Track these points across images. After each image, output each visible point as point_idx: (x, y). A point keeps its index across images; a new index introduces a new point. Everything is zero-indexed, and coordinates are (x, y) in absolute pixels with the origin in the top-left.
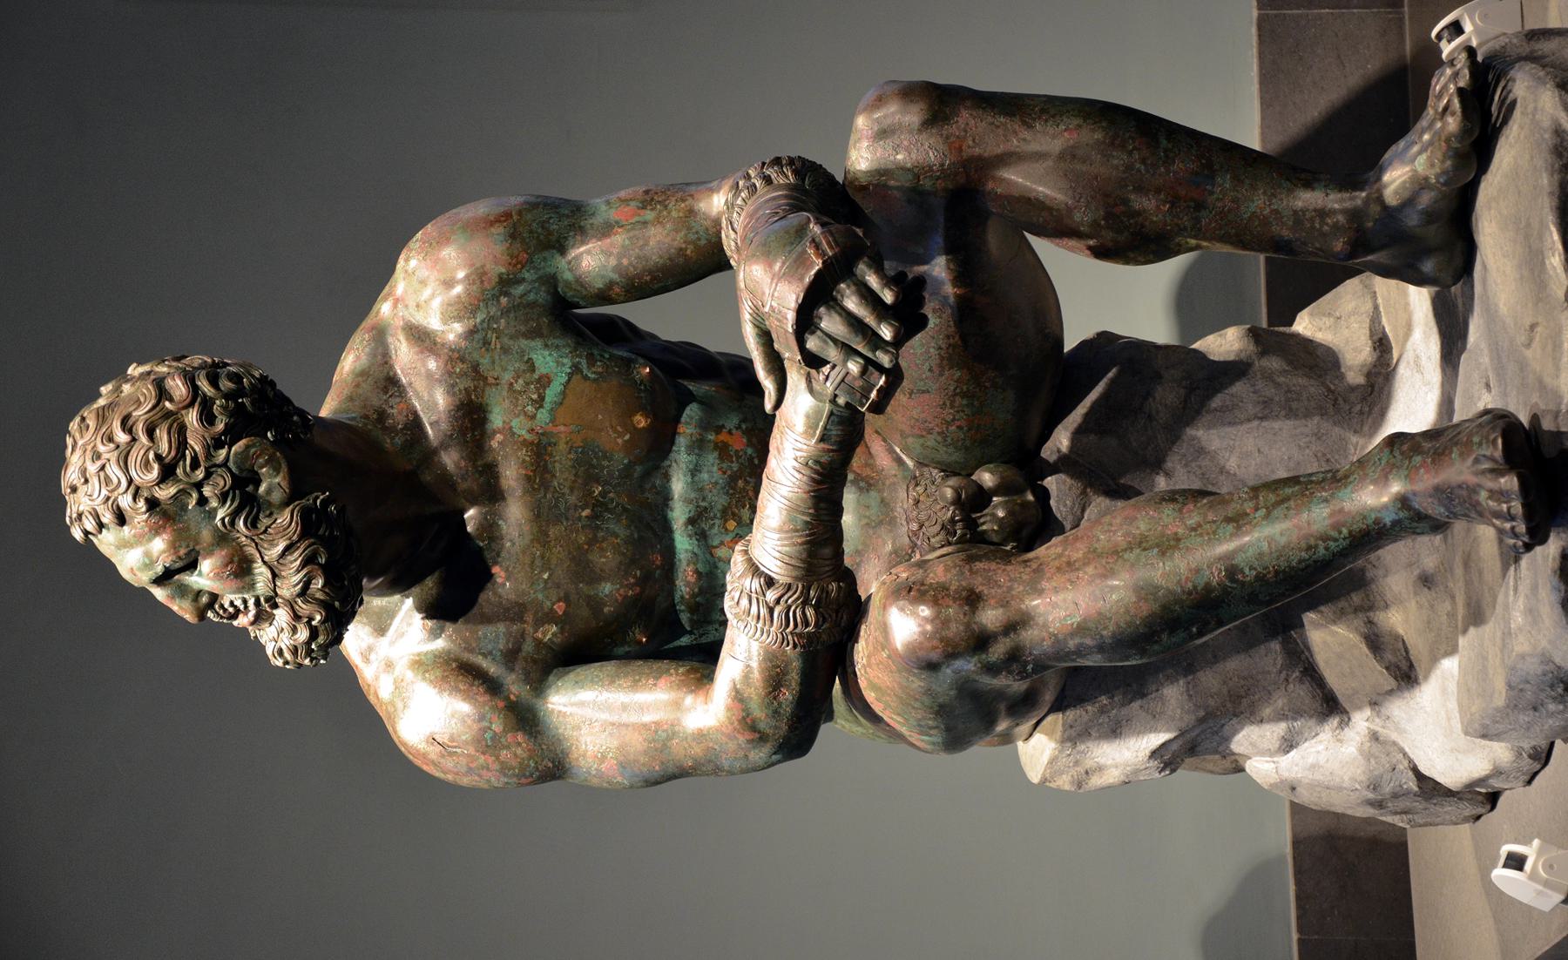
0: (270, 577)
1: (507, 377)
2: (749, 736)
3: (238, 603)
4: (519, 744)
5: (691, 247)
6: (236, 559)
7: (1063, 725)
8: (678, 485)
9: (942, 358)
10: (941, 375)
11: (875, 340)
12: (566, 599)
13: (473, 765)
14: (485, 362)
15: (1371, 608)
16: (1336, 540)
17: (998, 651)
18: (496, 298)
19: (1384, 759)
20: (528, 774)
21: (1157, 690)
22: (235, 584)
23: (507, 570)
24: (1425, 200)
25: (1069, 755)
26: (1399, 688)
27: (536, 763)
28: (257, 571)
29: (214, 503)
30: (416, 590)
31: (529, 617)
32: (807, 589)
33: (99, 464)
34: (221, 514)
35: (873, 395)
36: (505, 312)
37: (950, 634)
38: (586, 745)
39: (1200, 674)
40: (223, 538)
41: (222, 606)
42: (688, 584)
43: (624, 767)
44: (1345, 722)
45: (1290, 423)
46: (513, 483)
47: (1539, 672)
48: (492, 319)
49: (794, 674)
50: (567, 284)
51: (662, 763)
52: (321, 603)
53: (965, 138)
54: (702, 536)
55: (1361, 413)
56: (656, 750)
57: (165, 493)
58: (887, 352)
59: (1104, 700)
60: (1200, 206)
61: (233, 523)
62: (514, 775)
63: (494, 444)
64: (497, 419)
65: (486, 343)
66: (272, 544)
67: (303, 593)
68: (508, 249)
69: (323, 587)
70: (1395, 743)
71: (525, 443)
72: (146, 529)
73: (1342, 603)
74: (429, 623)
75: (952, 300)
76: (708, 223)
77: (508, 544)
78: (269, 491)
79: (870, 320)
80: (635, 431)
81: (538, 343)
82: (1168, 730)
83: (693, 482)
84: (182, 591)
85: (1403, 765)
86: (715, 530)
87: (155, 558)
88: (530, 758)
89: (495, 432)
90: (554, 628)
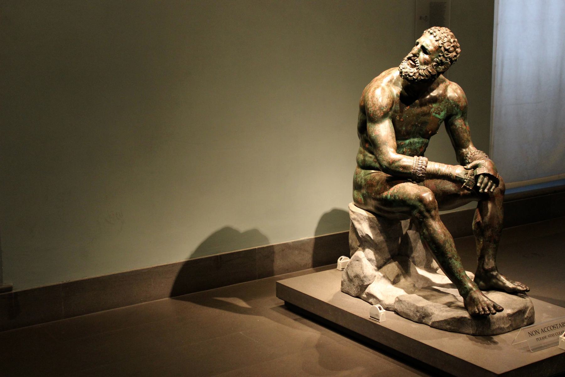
0: (424, 69)
1: (441, 107)
3: (418, 62)
5: (464, 142)
6: (428, 62)
7: (373, 217)
8: (416, 140)
9: (445, 191)
10: (441, 191)
11: (484, 188)
12: (403, 121)
13: (376, 105)
14: (443, 102)
15: (403, 275)
16: (460, 277)
17: (426, 214)
18: (455, 104)
19: (371, 278)
20: (374, 116)
21: (382, 235)
22: (422, 61)
23: (408, 109)
24: (500, 283)
25: (364, 218)
26: (391, 282)
28: (425, 66)
29: (440, 58)
30: (404, 91)
31: (401, 114)
32: (425, 174)
33: (447, 36)
34: (437, 59)
35: (468, 187)
36: (452, 106)
37: (430, 205)
39: (385, 243)
40: (432, 60)
41: (416, 59)
42: (401, 143)
44: (376, 270)
45: (425, 255)
46: (423, 109)
47: (429, 312)
48: (451, 103)
49: (406, 171)
50: (456, 117)
52: (417, 78)
53: (498, 197)
54: (408, 145)
55: (428, 268)
57: (442, 49)
58: (482, 190)
59: (379, 225)
60: (490, 242)
61: (435, 62)
62: (373, 113)
63: (430, 105)
64: (434, 105)
65: (446, 102)
66: (431, 69)
67: (420, 74)
68: (463, 106)
69: (421, 79)
70: (374, 280)
71: (430, 111)
73: (402, 269)
74: (399, 94)
75: (458, 193)
76: (468, 144)
77: (413, 109)
78: (439, 68)
79: (488, 187)
80: (429, 131)
81: (446, 112)
82: (373, 237)
83: (417, 142)
84: (419, 51)
85: (370, 282)
86: (408, 147)
88: (378, 116)
89: (432, 105)
90: (398, 119)
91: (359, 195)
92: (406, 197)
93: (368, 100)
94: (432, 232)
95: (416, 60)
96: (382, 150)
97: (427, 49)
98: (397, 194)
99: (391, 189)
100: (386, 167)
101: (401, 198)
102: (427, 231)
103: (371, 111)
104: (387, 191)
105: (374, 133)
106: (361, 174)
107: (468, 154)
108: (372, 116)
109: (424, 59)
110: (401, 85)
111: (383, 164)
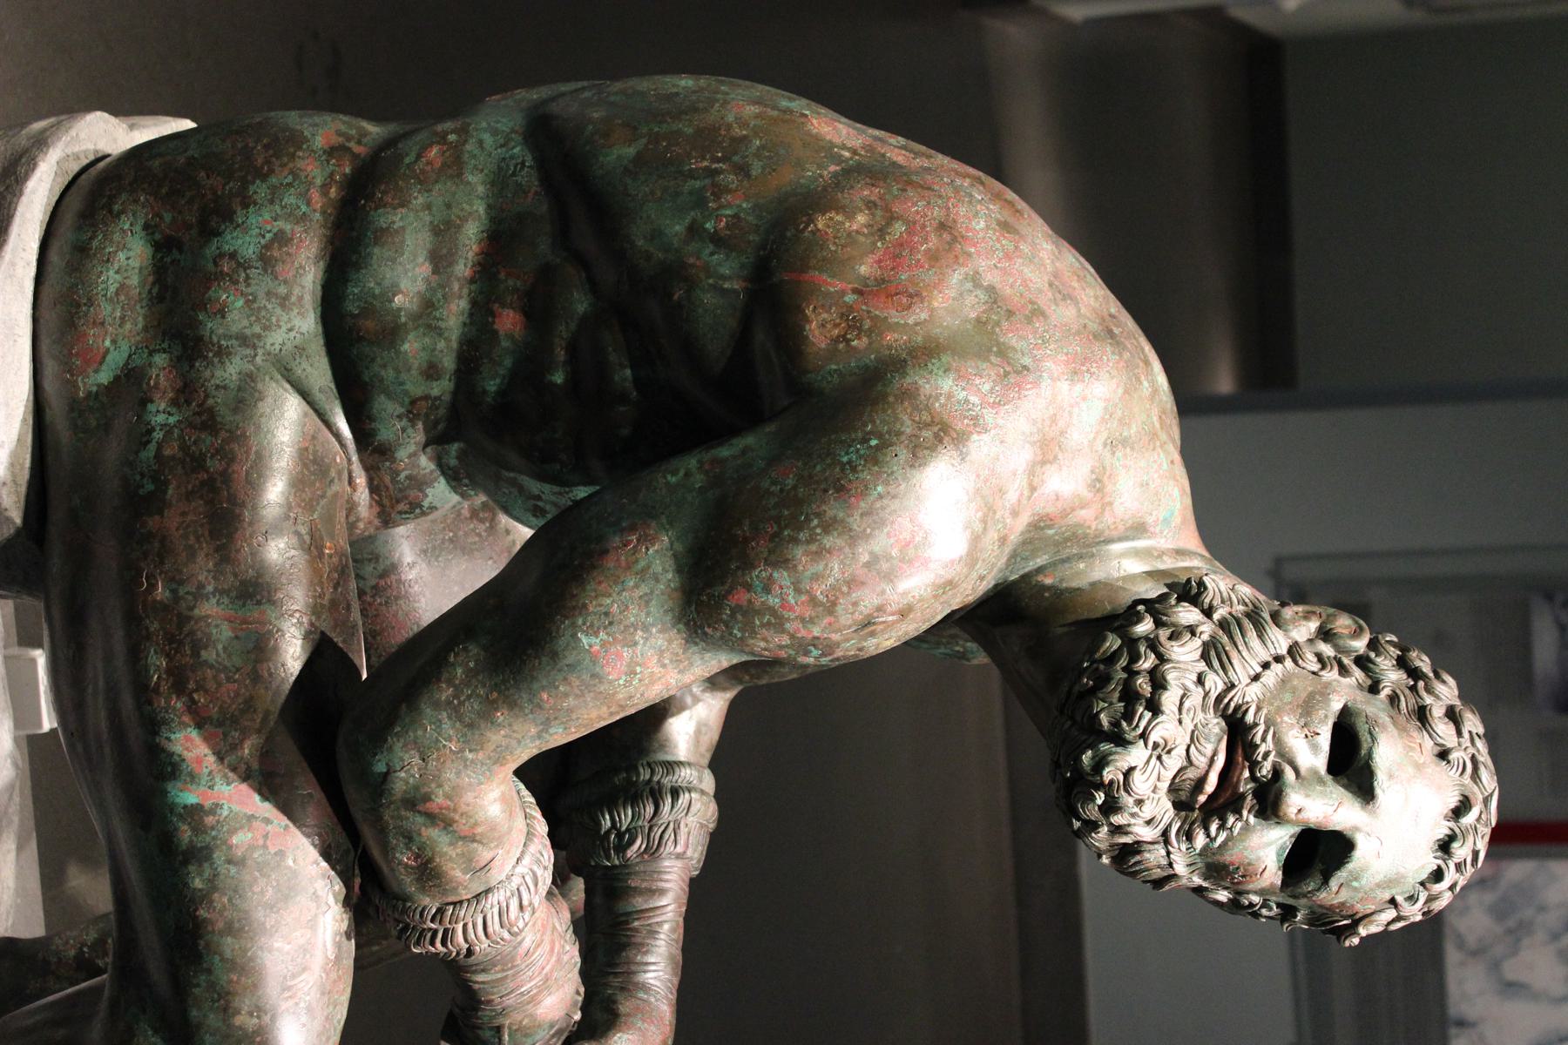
2: (432, 807)
4: (766, 649)
20: (739, 617)
22: (1229, 857)
27: (731, 634)
38: (664, 666)
43: (594, 676)
51: (540, 707)
56: (556, 718)
62: (759, 613)
87: (1343, 889)
91: (128, 326)
92: (223, 960)
93: (854, 539)
97: (1326, 881)
98: (222, 870)
99: (244, 787)
100: (386, 776)
101: (205, 920)
103: (767, 589)
104: (221, 759)
105: (604, 644)
106: (285, 318)
107: (675, 793)
108: (732, 602)
111: (390, 749)
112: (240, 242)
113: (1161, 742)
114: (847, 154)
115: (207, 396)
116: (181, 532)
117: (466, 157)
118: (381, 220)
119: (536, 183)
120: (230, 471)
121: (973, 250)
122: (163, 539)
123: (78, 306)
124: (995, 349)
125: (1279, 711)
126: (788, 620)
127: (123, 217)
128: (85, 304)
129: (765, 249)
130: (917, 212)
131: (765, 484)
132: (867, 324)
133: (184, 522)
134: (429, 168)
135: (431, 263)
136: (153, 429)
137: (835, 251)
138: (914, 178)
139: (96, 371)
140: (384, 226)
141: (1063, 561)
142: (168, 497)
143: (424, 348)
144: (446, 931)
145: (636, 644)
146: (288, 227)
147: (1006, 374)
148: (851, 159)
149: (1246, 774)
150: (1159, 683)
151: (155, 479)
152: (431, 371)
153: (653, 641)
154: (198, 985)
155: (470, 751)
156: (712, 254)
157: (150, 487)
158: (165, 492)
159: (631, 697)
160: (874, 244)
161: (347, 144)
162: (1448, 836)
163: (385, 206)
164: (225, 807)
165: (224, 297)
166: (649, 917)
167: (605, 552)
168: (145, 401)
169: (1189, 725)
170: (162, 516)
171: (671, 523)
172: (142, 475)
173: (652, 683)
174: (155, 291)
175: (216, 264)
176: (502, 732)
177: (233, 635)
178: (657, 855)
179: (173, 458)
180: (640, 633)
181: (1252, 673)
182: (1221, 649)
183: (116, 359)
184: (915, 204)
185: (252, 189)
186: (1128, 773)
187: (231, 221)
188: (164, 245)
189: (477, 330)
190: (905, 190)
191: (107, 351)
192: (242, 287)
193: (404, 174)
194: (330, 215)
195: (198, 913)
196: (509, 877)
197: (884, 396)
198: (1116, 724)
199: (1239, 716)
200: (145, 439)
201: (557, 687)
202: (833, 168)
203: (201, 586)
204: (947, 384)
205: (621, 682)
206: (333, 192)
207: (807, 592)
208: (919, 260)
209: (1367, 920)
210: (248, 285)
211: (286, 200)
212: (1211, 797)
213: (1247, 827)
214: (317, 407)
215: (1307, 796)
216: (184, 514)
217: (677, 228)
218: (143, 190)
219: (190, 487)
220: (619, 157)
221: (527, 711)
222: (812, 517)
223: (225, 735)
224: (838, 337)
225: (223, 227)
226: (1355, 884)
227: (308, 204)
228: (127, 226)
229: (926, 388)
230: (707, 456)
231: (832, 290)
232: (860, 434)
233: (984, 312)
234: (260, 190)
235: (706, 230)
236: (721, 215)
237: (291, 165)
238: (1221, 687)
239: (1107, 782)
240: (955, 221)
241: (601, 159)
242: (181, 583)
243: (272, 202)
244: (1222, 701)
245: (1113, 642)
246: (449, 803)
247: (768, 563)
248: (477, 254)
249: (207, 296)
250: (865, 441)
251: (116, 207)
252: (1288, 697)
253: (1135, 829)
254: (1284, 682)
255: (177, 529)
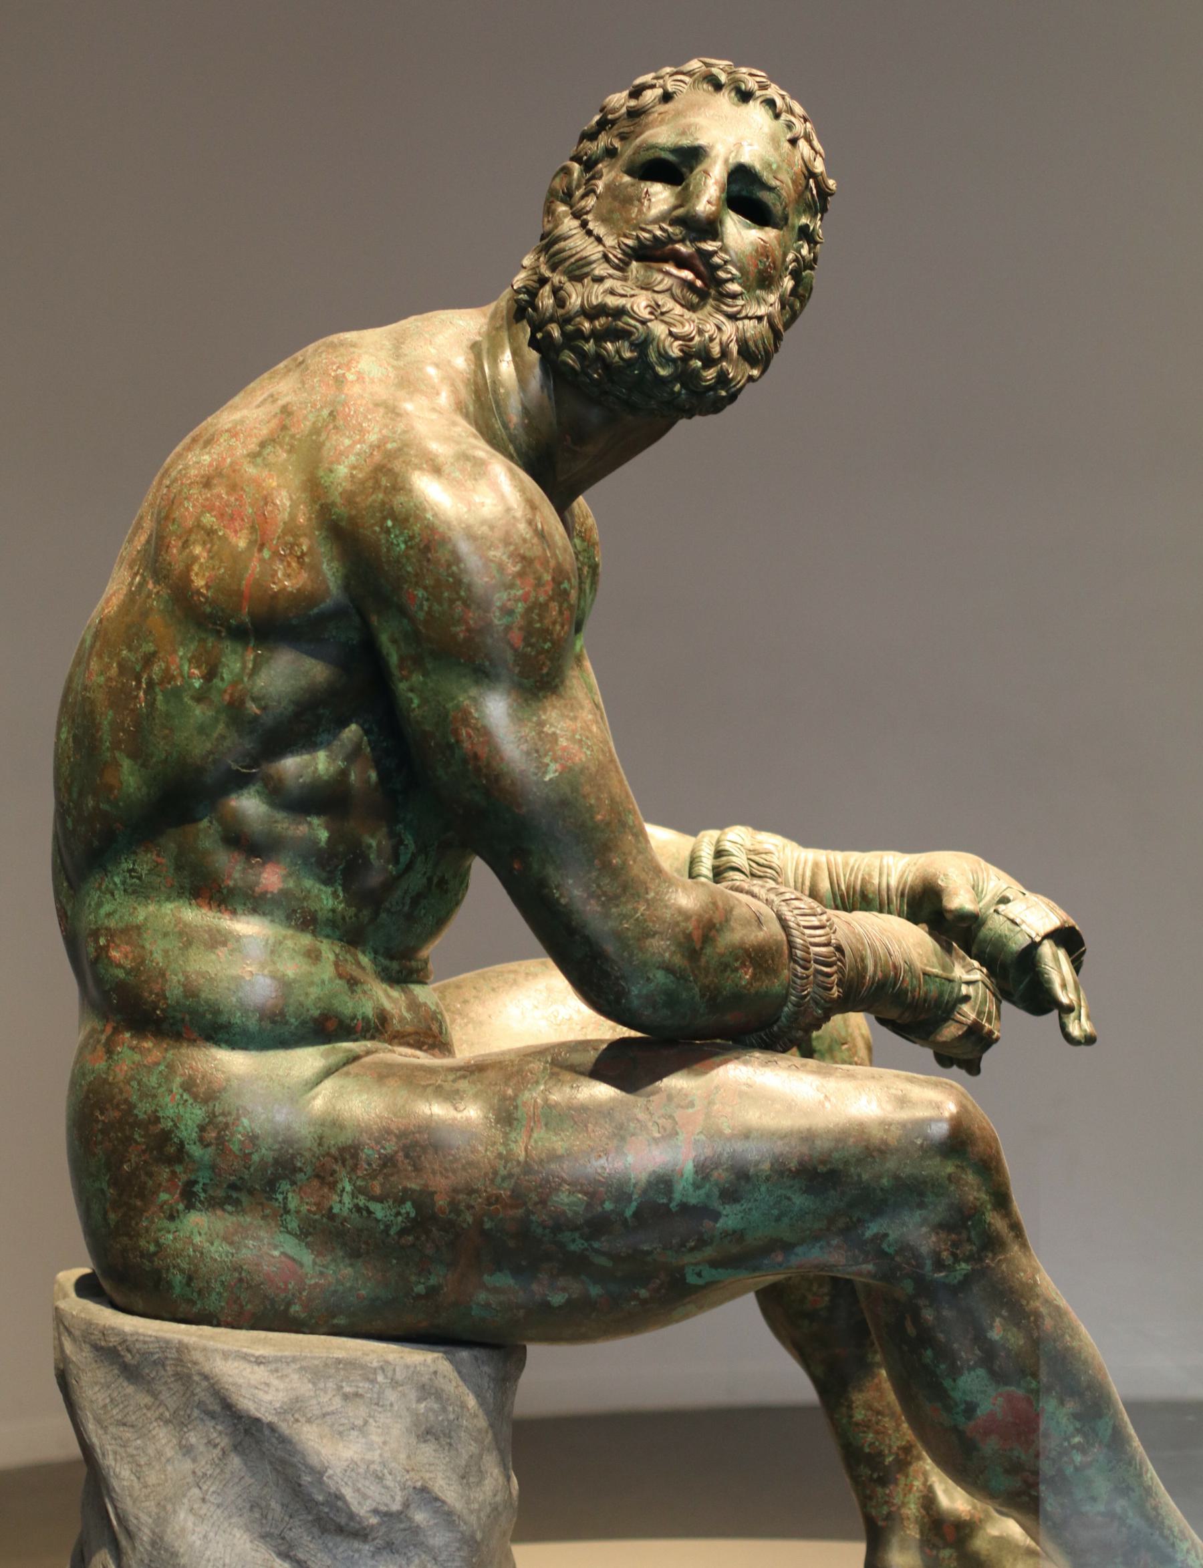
2: (697, 935)
4: (563, 626)
20: (533, 640)
27: (548, 651)
51: (608, 824)
62: (530, 623)
72: (795, 168)
87: (779, 176)
94: (1048, 1323)
95: (716, 260)
96: (625, 862)
101: (800, 1163)
102: (1018, 1325)
103: (510, 612)
105: (555, 760)
109: (763, 252)
110: (505, 437)
112: (190, 1122)
113: (649, 309)
114: (138, 579)
115: (328, 1154)
116: (450, 1174)
117: (121, 925)
118: (176, 992)
119: (149, 855)
120: (397, 1132)
121: (229, 460)
122: (455, 1191)
123: (241, 1280)
124: (314, 437)
125: (627, 221)
126: (537, 598)
127: (162, 1241)
128: (240, 1274)
129: (219, 632)
130: (194, 506)
131: (421, 616)
132: (290, 539)
133: (441, 1173)
134: (130, 956)
135: (216, 948)
136: (357, 1206)
137: (226, 568)
138: (163, 514)
139: (302, 1265)
140: (181, 989)
141: (498, 406)
142: (418, 1188)
143: (293, 958)
144: (816, 962)
145: (554, 733)
146: (178, 1080)
147: (335, 427)
148: (142, 575)
149: (679, 246)
150: (601, 310)
151: (401, 1201)
152: (313, 955)
153: (552, 720)
154: (859, 1176)
155: (647, 893)
156: (222, 679)
157: (408, 1205)
158: (413, 1191)
159: (602, 751)
160: (220, 538)
161: (103, 1041)
162: (736, 94)
163: (163, 991)
164: (697, 1137)
165: (239, 1136)
166: (838, 876)
167: (476, 757)
168: (331, 1216)
169: (637, 291)
170: (435, 1192)
171: (453, 699)
172: (398, 1214)
173: (591, 731)
174: (229, 1208)
175: (207, 1146)
176: (631, 863)
177: (544, 1128)
178: (779, 870)
179: (382, 1185)
180: (545, 729)
181: (596, 243)
182: (574, 266)
183: (291, 1246)
184: (187, 509)
185: (141, 1116)
186: (676, 337)
187: (170, 1132)
188: (189, 1198)
189: (278, 909)
190: (174, 520)
191: (284, 1254)
192: (230, 1119)
193: (135, 976)
194: (168, 1044)
195: (793, 1169)
196: (768, 902)
197: (351, 519)
198: (634, 346)
199: (629, 251)
200: (365, 1213)
201: (591, 805)
202: (150, 586)
203: (500, 1156)
204: (342, 470)
205: (589, 753)
206: (148, 1044)
207: (514, 577)
208: (236, 500)
209: (808, 164)
210: (230, 1113)
211: (153, 1084)
212: (698, 275)
213: (724, 249)
214: (341, 1064)
215: (698, 197)
216: (434, 1173)
217: (198, 712)
218: (137, 1224)
219: (410, 1168)
220: (131, 774)
221: (612, 836)
222: (450, 571)
223: (633, 1135)
224: (299, 562)
225: (175, 1140)
226: (774, 166)
227: (157, 1064)
228: (171, 1237)
229: (347, 485)
230: (396, 672)
231: (258, 569)
232: (383, 536)
233: (282, 447)
234: (143, 1109)
235: (201, 687)
236: (188, 673)
237: (121, 1084)
238: (606, 265)
239: (681, 354)
240: (203, 477)
241: (132, 790)
242: (495, 1173)
243: (154, 1096)
244: (617, 265)
245: (569, 358)
246: (693, 919)
247: (487, 611)
248: (210, 909)
249: (237, 1153)
250: (388, 531)
251: (152, 1248)
252: (616, 216)
253: (725, 338)
254: (604, 220)
255: (447, 1178)
